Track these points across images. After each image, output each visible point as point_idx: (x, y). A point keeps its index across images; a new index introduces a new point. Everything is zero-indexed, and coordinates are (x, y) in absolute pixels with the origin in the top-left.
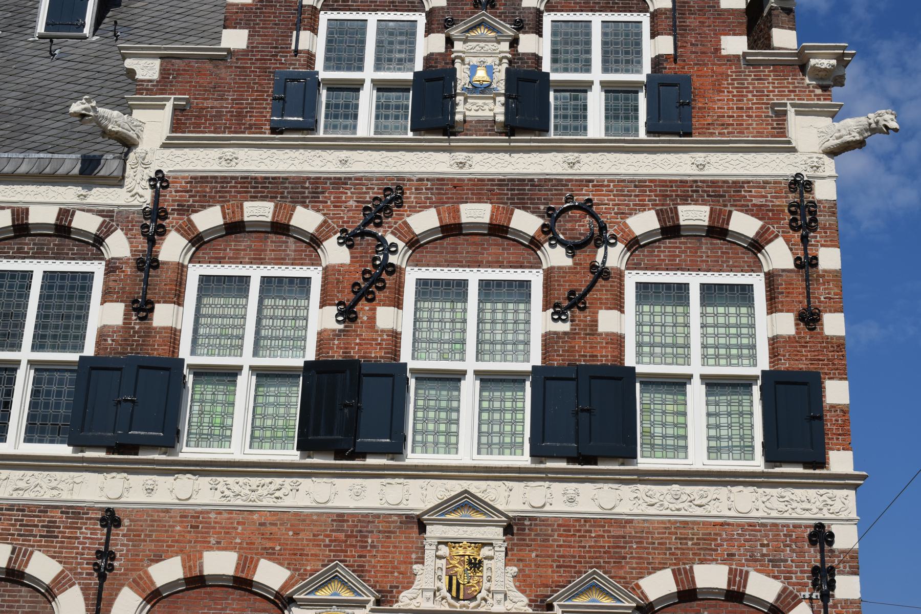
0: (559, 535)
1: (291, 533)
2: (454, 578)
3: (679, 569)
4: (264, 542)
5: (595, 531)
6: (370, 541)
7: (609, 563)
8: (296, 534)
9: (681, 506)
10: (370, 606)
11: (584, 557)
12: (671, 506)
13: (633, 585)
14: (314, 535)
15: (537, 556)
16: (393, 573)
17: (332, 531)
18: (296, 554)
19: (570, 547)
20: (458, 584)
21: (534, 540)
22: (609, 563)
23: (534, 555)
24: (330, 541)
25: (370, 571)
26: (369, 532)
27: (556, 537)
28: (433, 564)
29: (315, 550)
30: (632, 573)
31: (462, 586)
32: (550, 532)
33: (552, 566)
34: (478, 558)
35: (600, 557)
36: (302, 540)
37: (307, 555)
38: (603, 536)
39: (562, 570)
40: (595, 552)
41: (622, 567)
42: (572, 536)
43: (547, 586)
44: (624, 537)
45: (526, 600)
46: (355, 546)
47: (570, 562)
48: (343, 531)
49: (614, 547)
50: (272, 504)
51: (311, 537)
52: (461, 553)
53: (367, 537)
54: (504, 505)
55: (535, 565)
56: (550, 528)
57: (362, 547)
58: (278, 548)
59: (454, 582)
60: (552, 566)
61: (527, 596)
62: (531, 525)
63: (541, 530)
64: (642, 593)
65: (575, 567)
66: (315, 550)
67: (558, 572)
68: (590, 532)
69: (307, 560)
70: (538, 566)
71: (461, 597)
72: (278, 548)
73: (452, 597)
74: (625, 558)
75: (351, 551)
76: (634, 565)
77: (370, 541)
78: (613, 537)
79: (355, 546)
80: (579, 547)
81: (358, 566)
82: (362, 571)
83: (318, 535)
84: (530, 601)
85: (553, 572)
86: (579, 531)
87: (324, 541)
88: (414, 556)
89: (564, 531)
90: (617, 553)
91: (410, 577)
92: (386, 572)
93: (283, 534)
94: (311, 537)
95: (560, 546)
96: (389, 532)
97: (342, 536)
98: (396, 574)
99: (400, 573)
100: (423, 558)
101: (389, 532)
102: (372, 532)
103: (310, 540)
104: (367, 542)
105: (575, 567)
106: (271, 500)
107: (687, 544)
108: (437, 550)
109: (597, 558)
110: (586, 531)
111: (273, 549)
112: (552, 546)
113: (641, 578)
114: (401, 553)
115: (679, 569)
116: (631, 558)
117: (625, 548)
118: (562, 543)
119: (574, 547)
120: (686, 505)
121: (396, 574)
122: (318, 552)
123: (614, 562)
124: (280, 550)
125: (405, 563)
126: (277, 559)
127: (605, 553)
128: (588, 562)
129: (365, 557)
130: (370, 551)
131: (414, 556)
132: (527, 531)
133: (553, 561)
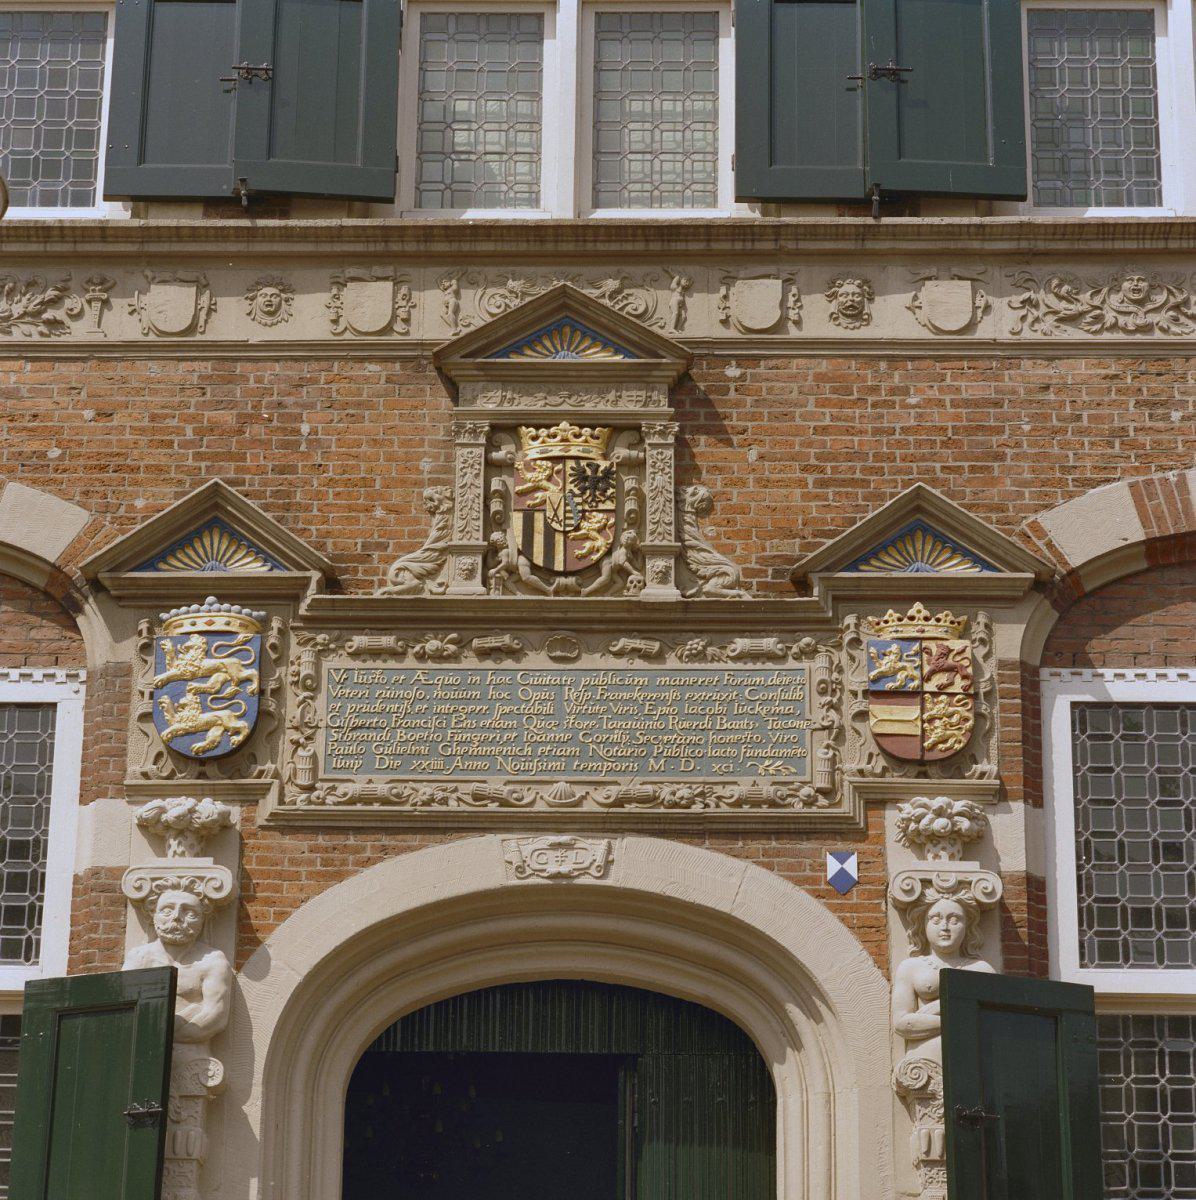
0: (820, 404)
1: (89, 414)
2: (539, 517)
3: (1149, 483)
4: (15, 438)
5: (918, 391)
6: (305, 428)
7: (958, 470)
8: (104, 415)
9: (1153, 318)
10: (312, 593)
11: (891, 458)
12: (1122, 320)
13: (1024, 525)
14: (153, 418)
15: (761, 457)
16: (368, 509)
17: (203, 406)
18: (103, 469)
19: (848, 431)
20: (550, 534)
21: (754, 417)
22: (958, 470)
23: (753, 455)
24: (196, 432)
25: (308, 508)
26: (305, 406)
27: (811, 407)
28: (480, 482)
29: (159, 457)
30: (1021, 495)
31: (559, 539)
32: (795, 395)
33: (802, 483)
34: (604, 464)
35: (933, 457)
36: (121, 429)
37: (134, 470)
38: (940, 403)
39: (830, 491)
40: (919, 444)
41: (993, 482)
42: (855, 403)
43: (791, 534)
44: (997, 404)
45: (733, 570)
46: (266, 444)
47: (852, 470)
48: (232, 405)
49: (971, 431)
50: (36, 338)
51: (146, 423)
52: (556, 452)
53: (299, 418)
54: (670, 327)
55: (758, 481)
56: (795, 386)
57: (285, 445)
58: (55, 453)
59: (539, 525)
60: (802, 483)
61: (738, 561)
62: (742, 377)
63: (770, 391)
64: (1050, 545)
65: (865, 483)
66: (159, 457)
67: (817, 497)
68: (905, 392)
69: (136, 483)
70: (763, 483)
71: (559, 566)
72: (55, 453)
73: (534, 568)
74: (1000, 457)
75: (255, 456)
76: (1027, 476)
77: (305, 428)
78: (967, 403)
79: (266, 444)
80: (877, 431)
81: (275, 494)
82: (287, 508)
83: (166, 417)
84: (748, 572)
85: (805, 497)
86: (875, 390)
87: (179, 431)
88: (426, 465)
89: (834, 391)
90: (979, 444)
91: (417, 521)
92: (350, 509)
93: (69, 417)
94: (146, 423)
95: (824, 430)
96: (359, 405)
97: (228, 417)
98: (379, 513)
99: (390, 510)
100: (452, 471)
101: (359, 405)
102: (312, 406)
103: (142, 431)
104: (298, 432)
105: (865, 483)
106: (33, 330)
107: (1166, 418)
108: (491, 445)
109: (923, 458)
110: (893, 391)
111: (43, 455)
112: (798, 431)
113: (1047, 507)
114: (390, 458)
115: (1149, 483)
116: (1016, 457)
117: (1000, 431)
118: (827, 422)
119: (861, 432)
120: (1162, 318)
121: (379, 513)
122: (163, 461)
123: (972, 469)
124: (61, 458)
125: (403, 482)
126: (54, 481)
127: (944, 444)
128: (899, 471)
129: (293, 470)
130: (306, 455)
131: (426, 465)
132: (732, 394)
133: (805, 469)
